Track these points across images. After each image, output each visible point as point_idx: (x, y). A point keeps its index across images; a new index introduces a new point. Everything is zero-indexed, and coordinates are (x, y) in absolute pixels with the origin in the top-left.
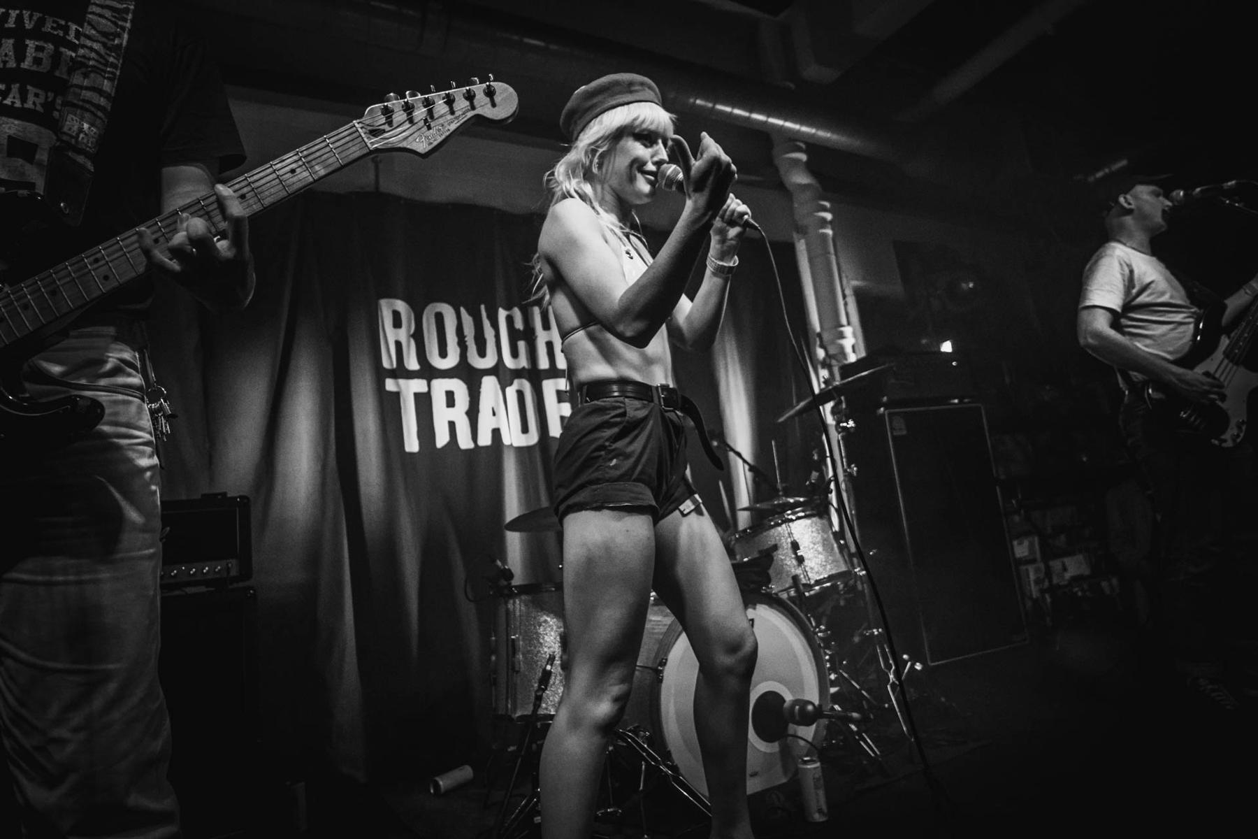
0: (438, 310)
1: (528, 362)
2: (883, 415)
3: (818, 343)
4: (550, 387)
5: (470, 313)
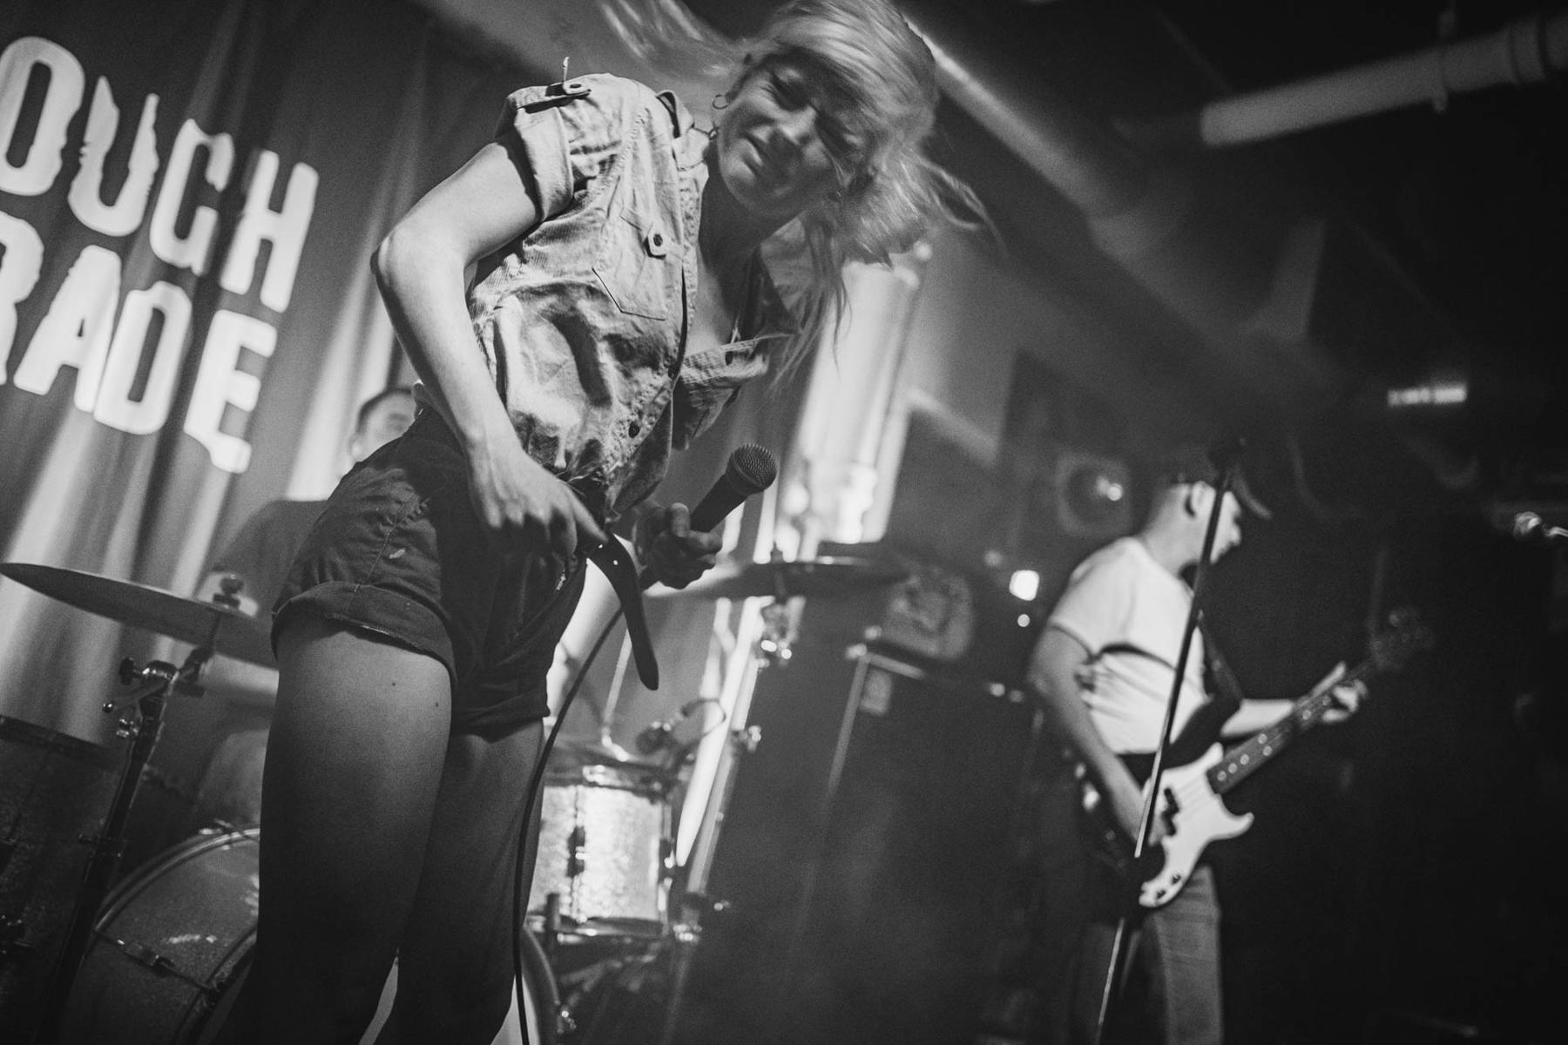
4: (228, 330)
5: (118, 100)
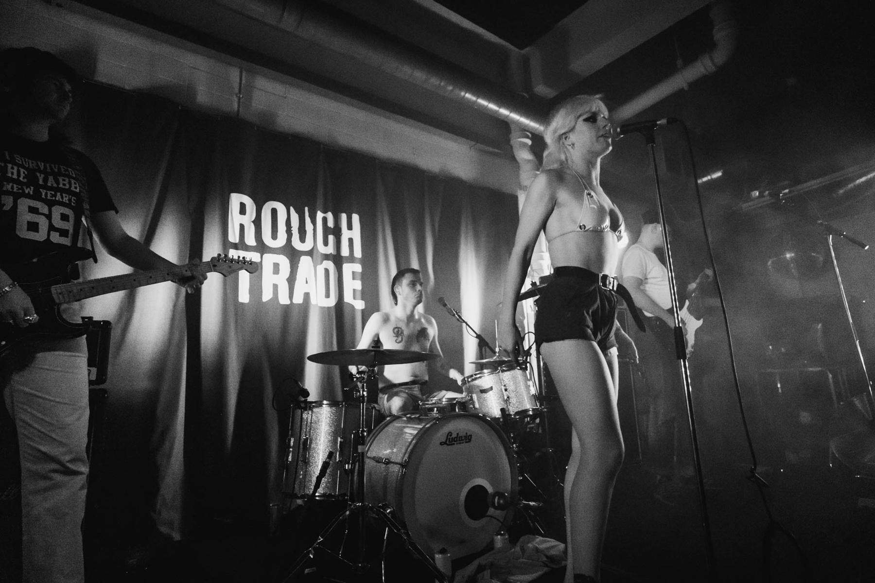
0: (274, 207)
1: (334, 250)
4: (348, 269)
5: (297, 212)
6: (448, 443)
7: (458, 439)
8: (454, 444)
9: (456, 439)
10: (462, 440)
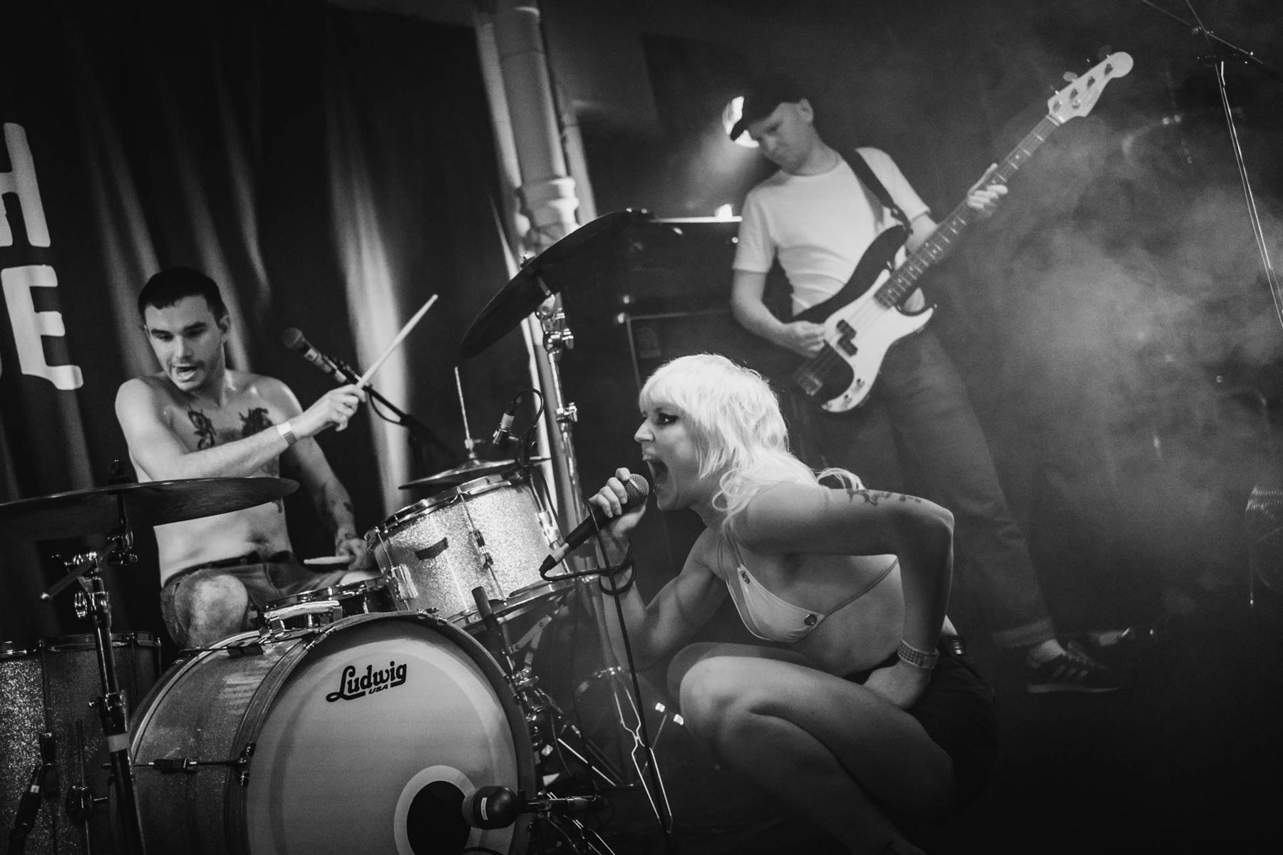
2: (625, 323)
3: (518, 206)
6: (346, 692)
7: (372, 681)
8: (363, 694)
9: (366, 682)
10: (382, 681)
